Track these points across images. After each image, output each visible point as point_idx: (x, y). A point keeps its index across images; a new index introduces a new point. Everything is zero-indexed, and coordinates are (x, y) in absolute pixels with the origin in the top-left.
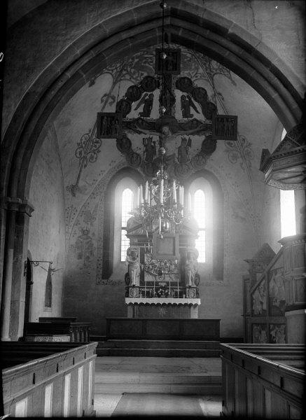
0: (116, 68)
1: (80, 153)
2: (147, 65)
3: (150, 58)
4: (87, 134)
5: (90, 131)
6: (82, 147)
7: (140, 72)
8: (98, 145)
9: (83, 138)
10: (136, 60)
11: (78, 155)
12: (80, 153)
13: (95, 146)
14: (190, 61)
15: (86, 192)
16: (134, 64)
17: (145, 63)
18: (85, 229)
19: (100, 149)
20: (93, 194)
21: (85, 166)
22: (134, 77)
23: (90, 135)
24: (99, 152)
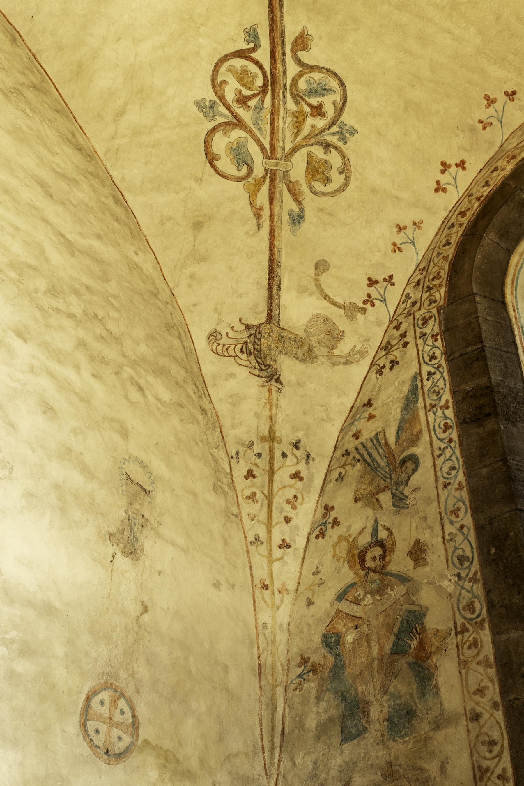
4: (239, 54)
6: (239, 123)
18: (365, 539)
19: (345, 118)
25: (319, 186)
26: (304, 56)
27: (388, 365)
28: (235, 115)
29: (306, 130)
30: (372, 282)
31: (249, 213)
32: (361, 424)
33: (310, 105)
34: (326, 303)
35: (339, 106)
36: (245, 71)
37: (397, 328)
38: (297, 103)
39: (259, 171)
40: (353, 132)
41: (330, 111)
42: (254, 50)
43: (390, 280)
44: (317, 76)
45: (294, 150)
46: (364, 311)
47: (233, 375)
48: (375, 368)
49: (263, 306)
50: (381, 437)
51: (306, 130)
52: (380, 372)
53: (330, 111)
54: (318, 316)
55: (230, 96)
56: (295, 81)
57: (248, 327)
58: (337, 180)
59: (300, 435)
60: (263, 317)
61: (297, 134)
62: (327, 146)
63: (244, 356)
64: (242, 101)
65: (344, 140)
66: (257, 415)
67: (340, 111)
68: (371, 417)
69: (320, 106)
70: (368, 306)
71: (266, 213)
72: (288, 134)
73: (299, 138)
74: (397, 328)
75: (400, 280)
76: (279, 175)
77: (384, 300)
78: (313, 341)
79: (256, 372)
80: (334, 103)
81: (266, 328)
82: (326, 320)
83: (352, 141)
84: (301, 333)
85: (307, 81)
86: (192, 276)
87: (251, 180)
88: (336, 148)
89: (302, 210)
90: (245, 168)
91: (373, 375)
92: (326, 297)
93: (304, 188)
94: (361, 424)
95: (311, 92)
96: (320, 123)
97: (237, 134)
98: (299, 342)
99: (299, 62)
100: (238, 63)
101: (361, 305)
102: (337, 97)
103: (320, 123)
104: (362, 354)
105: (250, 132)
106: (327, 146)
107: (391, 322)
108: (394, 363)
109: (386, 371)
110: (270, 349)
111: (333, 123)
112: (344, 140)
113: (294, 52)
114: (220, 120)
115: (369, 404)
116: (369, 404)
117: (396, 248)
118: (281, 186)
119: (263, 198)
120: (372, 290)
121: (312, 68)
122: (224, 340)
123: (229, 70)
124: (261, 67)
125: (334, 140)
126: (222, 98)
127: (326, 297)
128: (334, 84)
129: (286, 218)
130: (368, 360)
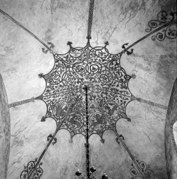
0: (59, 119)
2: (77, 120)
3: (79, 116)
4: (34, 162)
5: (36, 160)
6: (27, 171)
7: (74, 125)
8: (40, 174)
9: (30, 164)
10: (71, 117)
13: (38, 175)
14: (101, 118)
16: (70, 119)
17: (76, 119)
22: (70, 127)
23: (36, 163)
26: (40, 166)
28: (28, 170)
29: (35, 177)
36: (33, 164)
38: (36, 172)
41: (39, 175)
42: (35, 162)
44: (40, 169)
51: (35, 177)
53: (39, 175)
55: (29, 167)
56: (38, 168)
61: (33, 176)
64: (30, 168)
67: (41, 176)
69: (38, 174)
72: (32, 176)
80: (40, 174)
96: (37, 176)
97: (26, 173)
100: (32, 163)
102: (41, 174)
103: (37, 176)
105: (28, 173)
113: (39, 165)
114: (26, 170)
121: (40, 168)
123: (31, 163)
124: (35, 165)
126: (28, 167)
128: (42, 172)
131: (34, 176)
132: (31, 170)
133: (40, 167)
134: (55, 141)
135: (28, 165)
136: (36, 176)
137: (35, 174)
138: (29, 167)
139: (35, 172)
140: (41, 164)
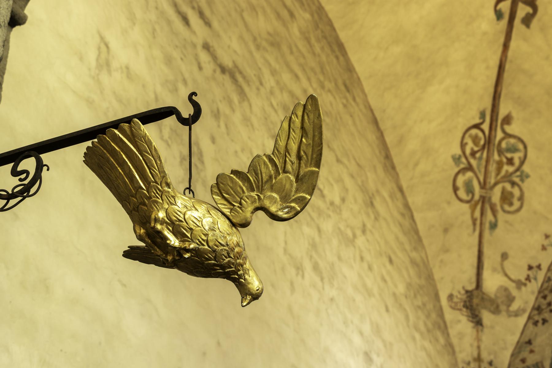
1: (469, 190)
4: (477, 126)
5: (483, 115)
6: (470, 168)
11: (462, 193)
12: (469, 190)
13: (510, 162)
15: (515, 307)
19: (526, 168)
20: (538, 309)
21: (494, 226)
23: (486, 127)
24: (524, 177)
25: (507, 208)
26: (508, 129)
27: (541, 322)
28: (469, 163)
29: (503, 173)
30: (530, 268)
31: (470, 222)
32: (525, 354)
33: (507, 158)
34: (505, 279)
35: (522, 159)
37: (545, 297)
39: (477, 197)
40: (528, 176)
41: (517, 162)
42: (482, 123)
43: (539, 267)
44: (512, 141)
45: (496, 184)
46: (525, 285)
47: (459, 321)
48: (531, 322)
49: (474, 279)
50: (540, 365)
51: (503, 173)
52: (536, 323)
53: (517, 162)
54: (501, 287)
55: (468, 151)
57: (467, 292)
58: (517, 204)
59: (492, 357)
60: (473, 286)
62: (513, 184)
63: (464, 310)
64: (473, 154)
65: (522, 180)
66: (471, 345)
67: (522, 163)
68: (532, 351)
70: (527, 282)
71: (478, 222)
73: (499, 177)
74: (545, 297)
75: (545, 267)
76: (487, 199)
77: (535, 279)
78: (499, 301)
79: (471, 319)
80: (520, 158)
81: (475, 293)
82: (506, 289)
83: (528, 182)
84: (493, 296)
85: (507, 144)
86: (442, 261)
87: (473, 202)
88: (518, 186)
89: (496, 221)
90: (470, 196)
91: (530, 325)
92: (506, 275)
93: (498, 208)
94: (525, 354)
95: (509, 150)
96: (511, 169)
97: (469, 174)
98: (492, 301)
99: (504, 131)
100: (474, 131)
101: (523, 280)
102: (521, 154)
103: (511, 169)
104: (524, 311)
106: (513, 184)
107: (539, 292)
108: (544, 321)
109: (540, 324)
110: (477, 305)
111: (517, 170)
112: (522, 180)
113: (502, 125)
114: (462, 166)
115: (529, 342)
116: (529, 342)
117: (544, 248)
118: (487, 207)
119: (477, 214)
120: (530, 273)
122: (455, 300)
123: (470, 136)
125: (517, 180)
127: (506, 275)
128: (521, 146)
129: (487, 225)
130: (526, 316)
131: (499, 169)
132: (481, 158)
133: (507, 135)
134: (530, 10)
135: (463, 145)
136: (507, 171)
137: (500, 165)
138: (468, 151)
139: (496, 157)
140: (507, 120)
